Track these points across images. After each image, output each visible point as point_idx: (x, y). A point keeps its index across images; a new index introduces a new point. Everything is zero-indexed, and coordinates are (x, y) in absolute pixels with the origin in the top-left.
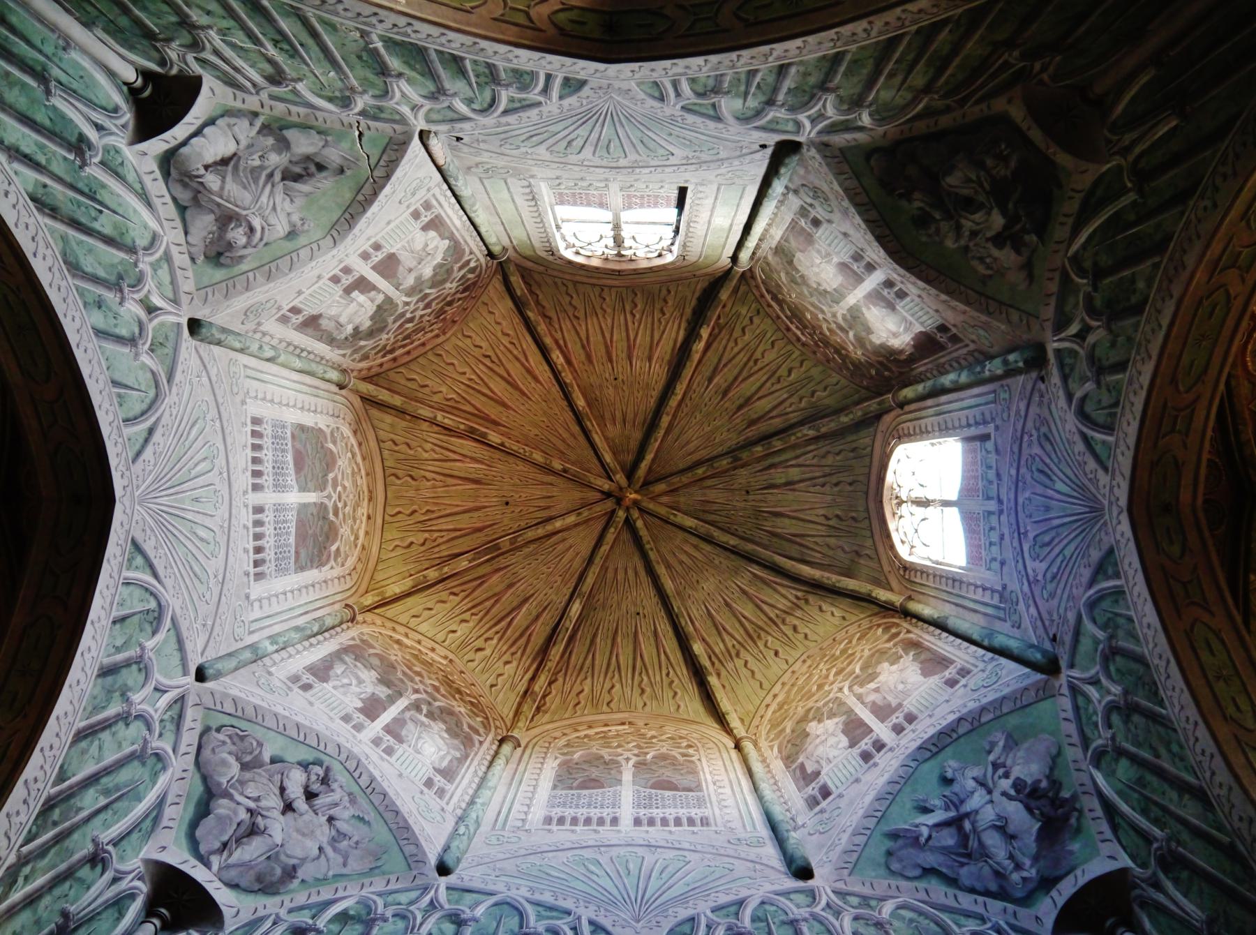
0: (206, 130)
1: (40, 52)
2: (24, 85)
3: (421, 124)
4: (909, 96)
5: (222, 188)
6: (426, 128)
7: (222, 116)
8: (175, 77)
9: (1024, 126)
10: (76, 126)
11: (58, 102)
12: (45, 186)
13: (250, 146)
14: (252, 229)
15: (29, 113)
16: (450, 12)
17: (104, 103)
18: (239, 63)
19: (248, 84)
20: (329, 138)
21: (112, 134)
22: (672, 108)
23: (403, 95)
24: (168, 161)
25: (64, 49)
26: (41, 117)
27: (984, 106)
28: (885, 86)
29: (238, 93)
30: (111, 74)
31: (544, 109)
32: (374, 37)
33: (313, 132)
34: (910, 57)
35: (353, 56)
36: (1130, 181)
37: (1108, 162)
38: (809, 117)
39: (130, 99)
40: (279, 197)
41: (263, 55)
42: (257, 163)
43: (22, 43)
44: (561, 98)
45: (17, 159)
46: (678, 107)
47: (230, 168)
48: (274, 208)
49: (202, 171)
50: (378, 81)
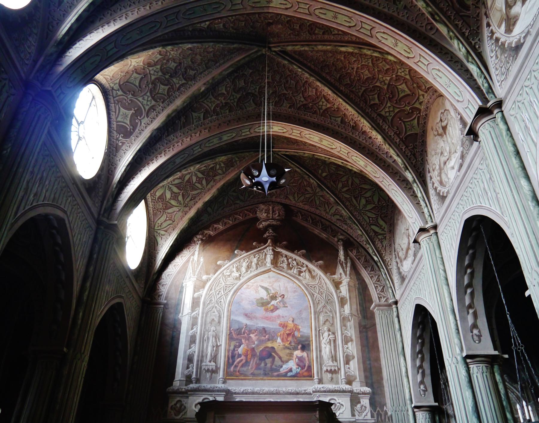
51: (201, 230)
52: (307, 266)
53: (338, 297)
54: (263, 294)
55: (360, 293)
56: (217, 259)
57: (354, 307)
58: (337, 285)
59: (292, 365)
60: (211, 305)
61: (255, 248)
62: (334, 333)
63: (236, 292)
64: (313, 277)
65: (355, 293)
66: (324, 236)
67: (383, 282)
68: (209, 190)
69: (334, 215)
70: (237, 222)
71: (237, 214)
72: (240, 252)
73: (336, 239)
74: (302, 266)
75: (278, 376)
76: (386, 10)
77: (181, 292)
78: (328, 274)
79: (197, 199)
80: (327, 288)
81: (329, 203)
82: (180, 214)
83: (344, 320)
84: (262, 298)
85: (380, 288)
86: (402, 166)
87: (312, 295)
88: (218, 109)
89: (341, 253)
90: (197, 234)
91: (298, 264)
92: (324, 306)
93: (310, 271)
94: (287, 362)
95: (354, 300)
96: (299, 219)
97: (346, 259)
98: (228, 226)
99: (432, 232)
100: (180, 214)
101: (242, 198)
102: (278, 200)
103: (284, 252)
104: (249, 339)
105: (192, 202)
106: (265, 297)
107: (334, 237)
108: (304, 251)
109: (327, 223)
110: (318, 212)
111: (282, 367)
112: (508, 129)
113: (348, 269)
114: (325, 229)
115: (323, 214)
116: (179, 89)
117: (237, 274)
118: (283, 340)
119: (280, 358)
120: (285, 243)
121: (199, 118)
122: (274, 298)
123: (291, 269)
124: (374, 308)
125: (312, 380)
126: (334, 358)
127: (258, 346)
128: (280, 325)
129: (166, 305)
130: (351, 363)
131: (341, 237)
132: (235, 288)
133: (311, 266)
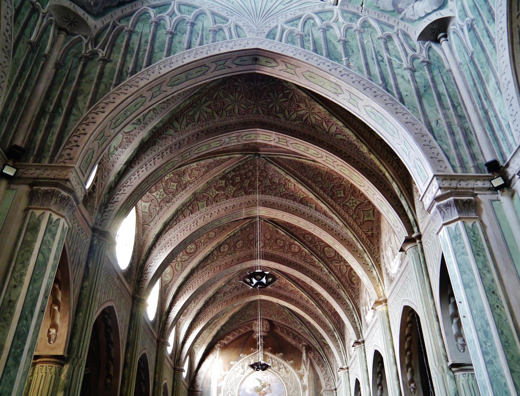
0: (423, 15)
1: (469, 68)
2: (479, 61)
3: (336, 9)
4: (137, 29)
6: (335, 7)
7: (415, 20)
8: (427, 41)
9: (87, 15)
10: (469, 36)
11: (471, 49)
12: (488, 22)
15: (481, 50)
16: (315, 72)
17: (457, 37)
18: (400, 49)
19: (400, 36)
20: (375, 4)
21: (459, 24)
22: (233, 19)
23: (340, 28)
25: (461, 64)
26: (478, 47)
27: (106, 23)
28: (147, 35)
29: (406, 31)
30: (450, 47)
31: (284, 20)
32: (345, 63)
33: (381, 8)
34: (141, 53)
35: (355, 52)
36: (38, 5)
37: (48, 7)
38: (176, 15)
39: (448, 33)
41: (389, 54)
43: (473, 74)
44: (277, 27)
45: (492, 38)
46: (230, 21)
50: (349, 39)
51: (219, 340)
53: (302, 385)
54: (258, 384)
55: (315, 382)
56: (230, 361)
57: (311, 391)
58: (301, 377)
60: (228, 392)
61: (253, 352)
63: (242, 383)
64: (287, 372)
65: (312, 382)
66: (294, 343)
67: (329, 375)
68: (224, 318)
69: (300, 329)
70: (241, 334)
71: (240, 328)
72: (244, 355)
73: (301, 345)
74: (281, 365)
76: (317, 273)
77: (210, 383)
78: (296, 370)
79: (217, 324)
80: (296, 379)
81: (296, 323)
82: (207, 333)
84: (257, 387)
85: (327, 379)
86: (332, 329)
87: (287, 384)
88: (231, 290)
89: (304, 355)
90: (217, 343)
91: (278, 363)
92: (294, 392)
93: (285, 368)
95: (311, 387)
96: (278, 331)
97: (307, 359)
98: (235, 337)
99: (346, 370)
100: (207, 333)
101: (243, 318)
102: (266, 318)
103: (270, 355)
105: (214, 326)
106: (259, 386)
107: (300, 343)
108: (281, 354)
109: (296, 334)
110: (290, 326)
112: (365, 357)
113: (308, 366)
114: (294, 338)
115: (293, 328)
116: (210, 286)
117: (242, 371)
120: (270, 348)
121: (221, 296)
122: (264, 386)
123: (274, 366)
129: (201, 392)
131: (304, 344)
132: (241, 380)
133: (286, 364)
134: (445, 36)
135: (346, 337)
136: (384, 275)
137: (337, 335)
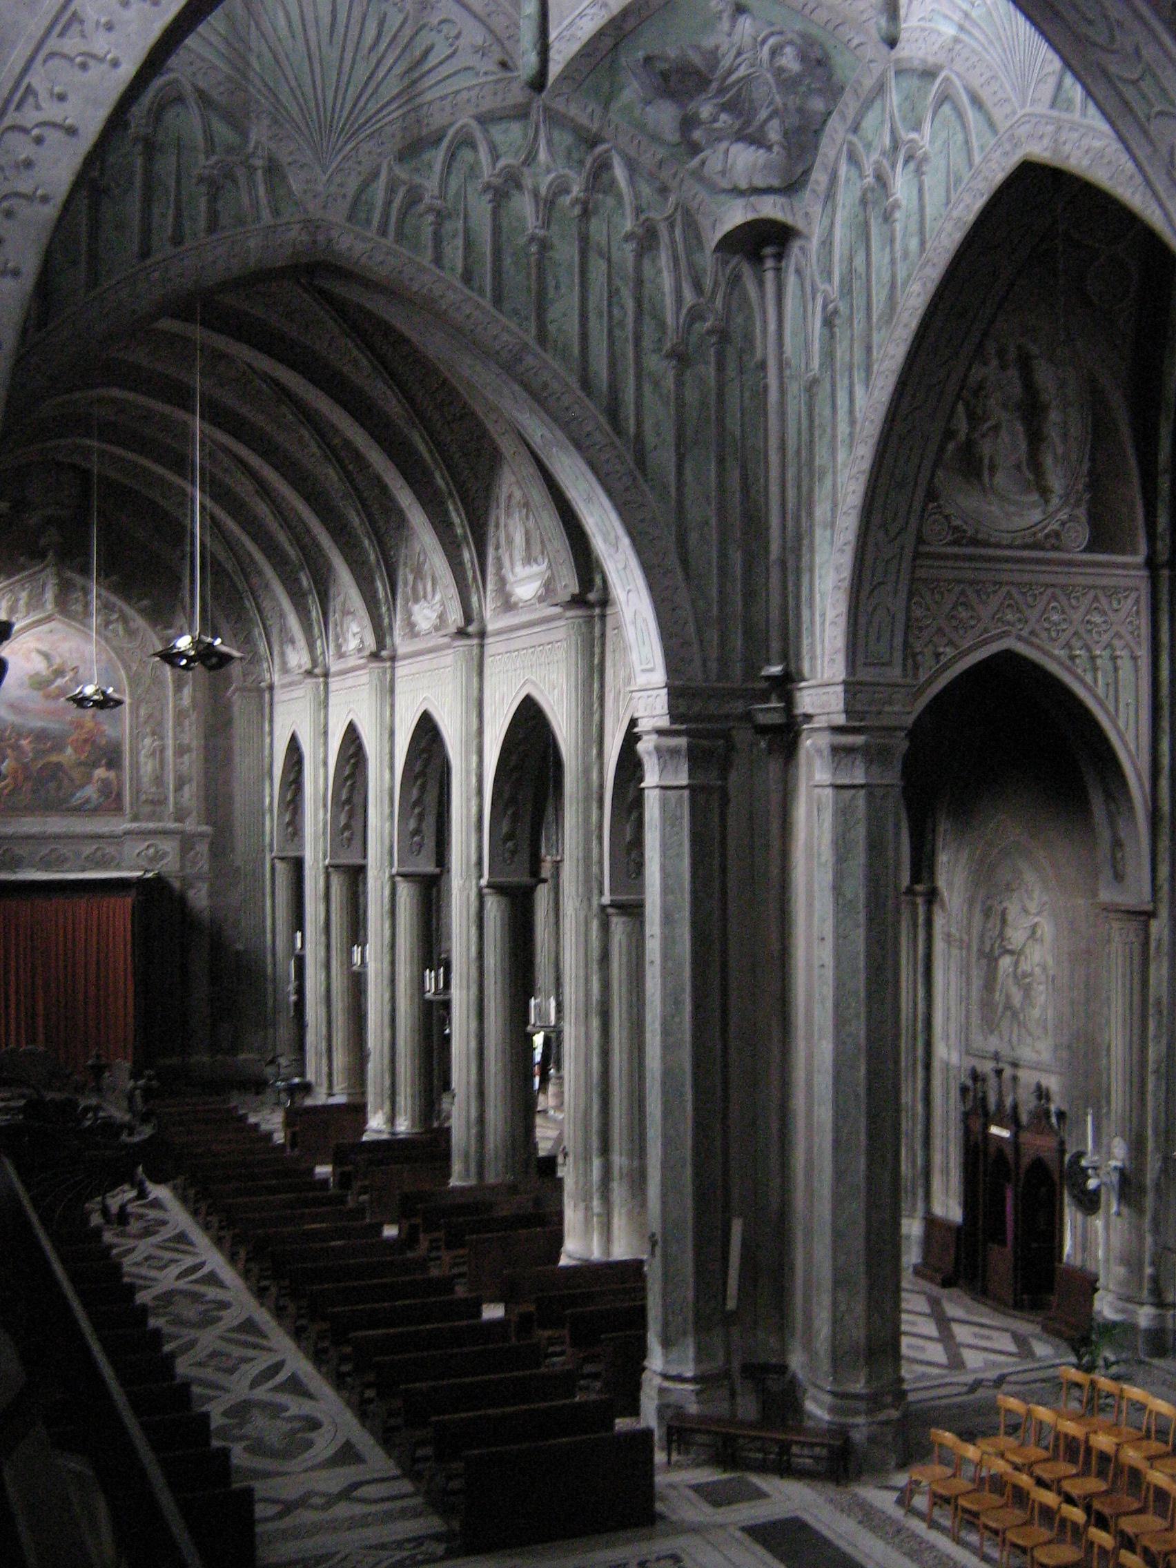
0: (743, 185)
5: (770, 118)
8: (735, 253)
13: (719, 140)
14: (774, 53)
24: (791, 187)
40: (725, 63)
42: (724, 117)
47: (749, 131)
48: (739, 54)
49: (776, 149)
52: (121, 611)
59: (91, 791)
62: (162, 738)
75: (68, 810)
83: (180, 715)
84: (37, 674)
94: (82, 786)
104: (17, 748)
111: (72, 795)
118: (75, 750)
119: (72, 780)
122: (59, 673)
124: (234, 693)
125: (124, 815)
126: (159, 780)
127: (34, 760)
128: (71, 723)
130: (186, 788)
133: (130, 612)
134: (779, 257)
135: (332, 592)
136: (490, 578)
137: (305, 581)
